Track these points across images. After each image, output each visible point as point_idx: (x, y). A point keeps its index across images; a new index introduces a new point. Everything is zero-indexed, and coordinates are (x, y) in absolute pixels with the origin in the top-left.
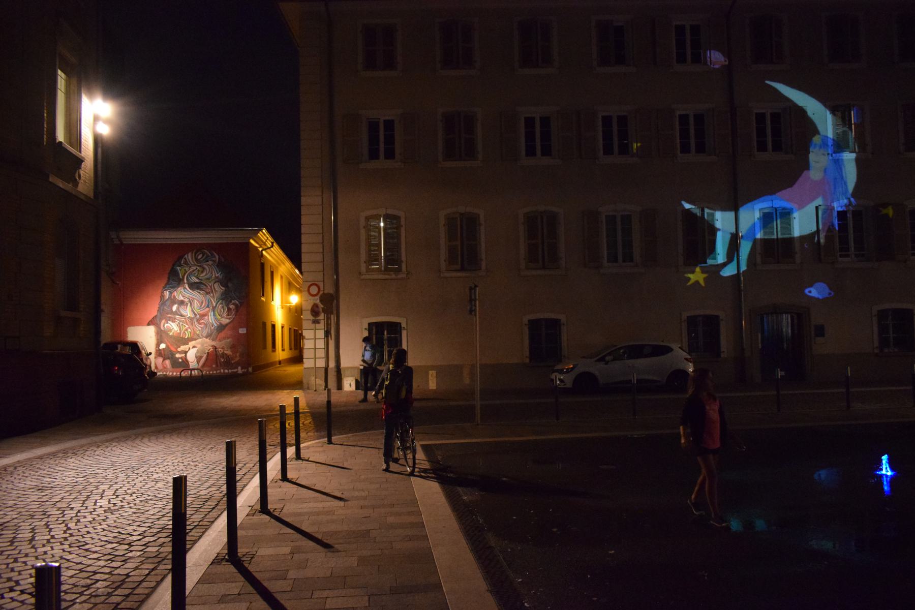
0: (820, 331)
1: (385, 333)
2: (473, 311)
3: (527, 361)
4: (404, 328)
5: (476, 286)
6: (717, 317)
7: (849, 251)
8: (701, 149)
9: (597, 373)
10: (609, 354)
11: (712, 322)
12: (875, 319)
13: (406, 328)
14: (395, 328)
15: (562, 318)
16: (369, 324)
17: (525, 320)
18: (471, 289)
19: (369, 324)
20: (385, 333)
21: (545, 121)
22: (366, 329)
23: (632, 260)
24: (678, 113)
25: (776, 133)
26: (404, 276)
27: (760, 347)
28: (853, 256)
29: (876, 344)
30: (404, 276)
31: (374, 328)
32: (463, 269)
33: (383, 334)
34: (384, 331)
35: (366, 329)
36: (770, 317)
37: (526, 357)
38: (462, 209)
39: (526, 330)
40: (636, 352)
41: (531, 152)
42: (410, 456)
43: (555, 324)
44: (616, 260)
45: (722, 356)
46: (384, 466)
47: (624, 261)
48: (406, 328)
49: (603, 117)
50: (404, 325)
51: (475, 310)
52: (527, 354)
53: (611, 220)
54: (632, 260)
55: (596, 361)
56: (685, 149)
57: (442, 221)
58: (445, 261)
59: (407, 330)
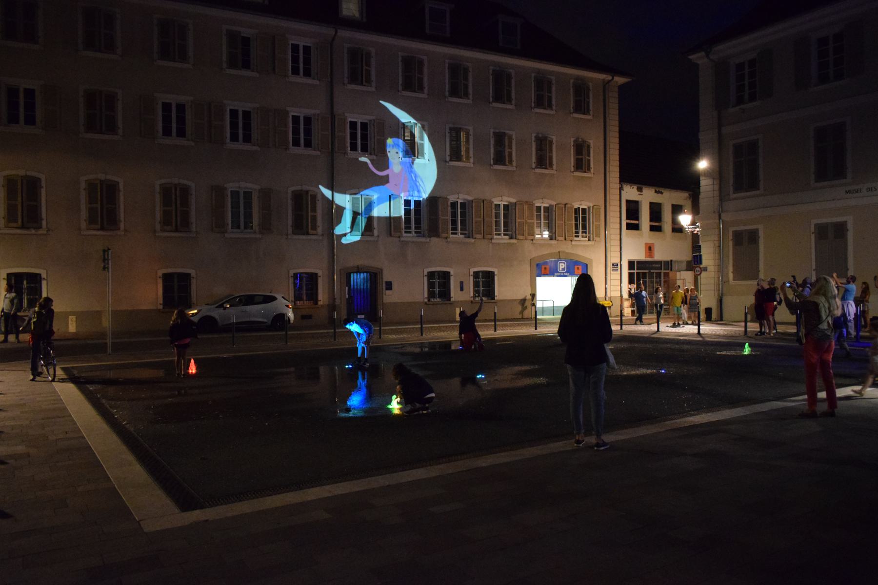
0: (389, 286)
1: (25, 282)
2: (106, 268)
3: (161, 307)
4: (44, 278)
5: (109, 249)
6: (316, 274)
7: (411, 229)
8: (308, 144)
9: (217, 317)
10: (227, 302)
11: (313, 278)
12: (426, 278)
13: (46, 278)
14: (35, 279)
15: (193, 272)
16: (9, 275)
17: (160, 273)
18: (104, 251)
19: (8, 275)
20: (25, 282)
21: (181, 108)
22: (4, 279)
24: (291, 114)
25: (364, 137)
26: (45, 232)
27: (347, 297)
28: (414, 233)
29: (426, 296)
30: (45, 232)
31: (13, 278)
32: (102, 228)
33: (22, 283)
34: (23, 281)
35: (4, 279)
36: (358, 276)
37: (160, 304)
38: (102, 177)
40: (250, 300)
41: (167, 132)
42: (51, 371)
43: (185, 278)
44: (239, 227)
46: (31, 377)
48: (46, 278)
49: (231, 110)
50: (44, 276)
51: (108, 268)
52: (162, 302)
53: (235, 194)
55: (217, 307)
56: (296, 143)
57: (83, 185)
59: (47, 280)
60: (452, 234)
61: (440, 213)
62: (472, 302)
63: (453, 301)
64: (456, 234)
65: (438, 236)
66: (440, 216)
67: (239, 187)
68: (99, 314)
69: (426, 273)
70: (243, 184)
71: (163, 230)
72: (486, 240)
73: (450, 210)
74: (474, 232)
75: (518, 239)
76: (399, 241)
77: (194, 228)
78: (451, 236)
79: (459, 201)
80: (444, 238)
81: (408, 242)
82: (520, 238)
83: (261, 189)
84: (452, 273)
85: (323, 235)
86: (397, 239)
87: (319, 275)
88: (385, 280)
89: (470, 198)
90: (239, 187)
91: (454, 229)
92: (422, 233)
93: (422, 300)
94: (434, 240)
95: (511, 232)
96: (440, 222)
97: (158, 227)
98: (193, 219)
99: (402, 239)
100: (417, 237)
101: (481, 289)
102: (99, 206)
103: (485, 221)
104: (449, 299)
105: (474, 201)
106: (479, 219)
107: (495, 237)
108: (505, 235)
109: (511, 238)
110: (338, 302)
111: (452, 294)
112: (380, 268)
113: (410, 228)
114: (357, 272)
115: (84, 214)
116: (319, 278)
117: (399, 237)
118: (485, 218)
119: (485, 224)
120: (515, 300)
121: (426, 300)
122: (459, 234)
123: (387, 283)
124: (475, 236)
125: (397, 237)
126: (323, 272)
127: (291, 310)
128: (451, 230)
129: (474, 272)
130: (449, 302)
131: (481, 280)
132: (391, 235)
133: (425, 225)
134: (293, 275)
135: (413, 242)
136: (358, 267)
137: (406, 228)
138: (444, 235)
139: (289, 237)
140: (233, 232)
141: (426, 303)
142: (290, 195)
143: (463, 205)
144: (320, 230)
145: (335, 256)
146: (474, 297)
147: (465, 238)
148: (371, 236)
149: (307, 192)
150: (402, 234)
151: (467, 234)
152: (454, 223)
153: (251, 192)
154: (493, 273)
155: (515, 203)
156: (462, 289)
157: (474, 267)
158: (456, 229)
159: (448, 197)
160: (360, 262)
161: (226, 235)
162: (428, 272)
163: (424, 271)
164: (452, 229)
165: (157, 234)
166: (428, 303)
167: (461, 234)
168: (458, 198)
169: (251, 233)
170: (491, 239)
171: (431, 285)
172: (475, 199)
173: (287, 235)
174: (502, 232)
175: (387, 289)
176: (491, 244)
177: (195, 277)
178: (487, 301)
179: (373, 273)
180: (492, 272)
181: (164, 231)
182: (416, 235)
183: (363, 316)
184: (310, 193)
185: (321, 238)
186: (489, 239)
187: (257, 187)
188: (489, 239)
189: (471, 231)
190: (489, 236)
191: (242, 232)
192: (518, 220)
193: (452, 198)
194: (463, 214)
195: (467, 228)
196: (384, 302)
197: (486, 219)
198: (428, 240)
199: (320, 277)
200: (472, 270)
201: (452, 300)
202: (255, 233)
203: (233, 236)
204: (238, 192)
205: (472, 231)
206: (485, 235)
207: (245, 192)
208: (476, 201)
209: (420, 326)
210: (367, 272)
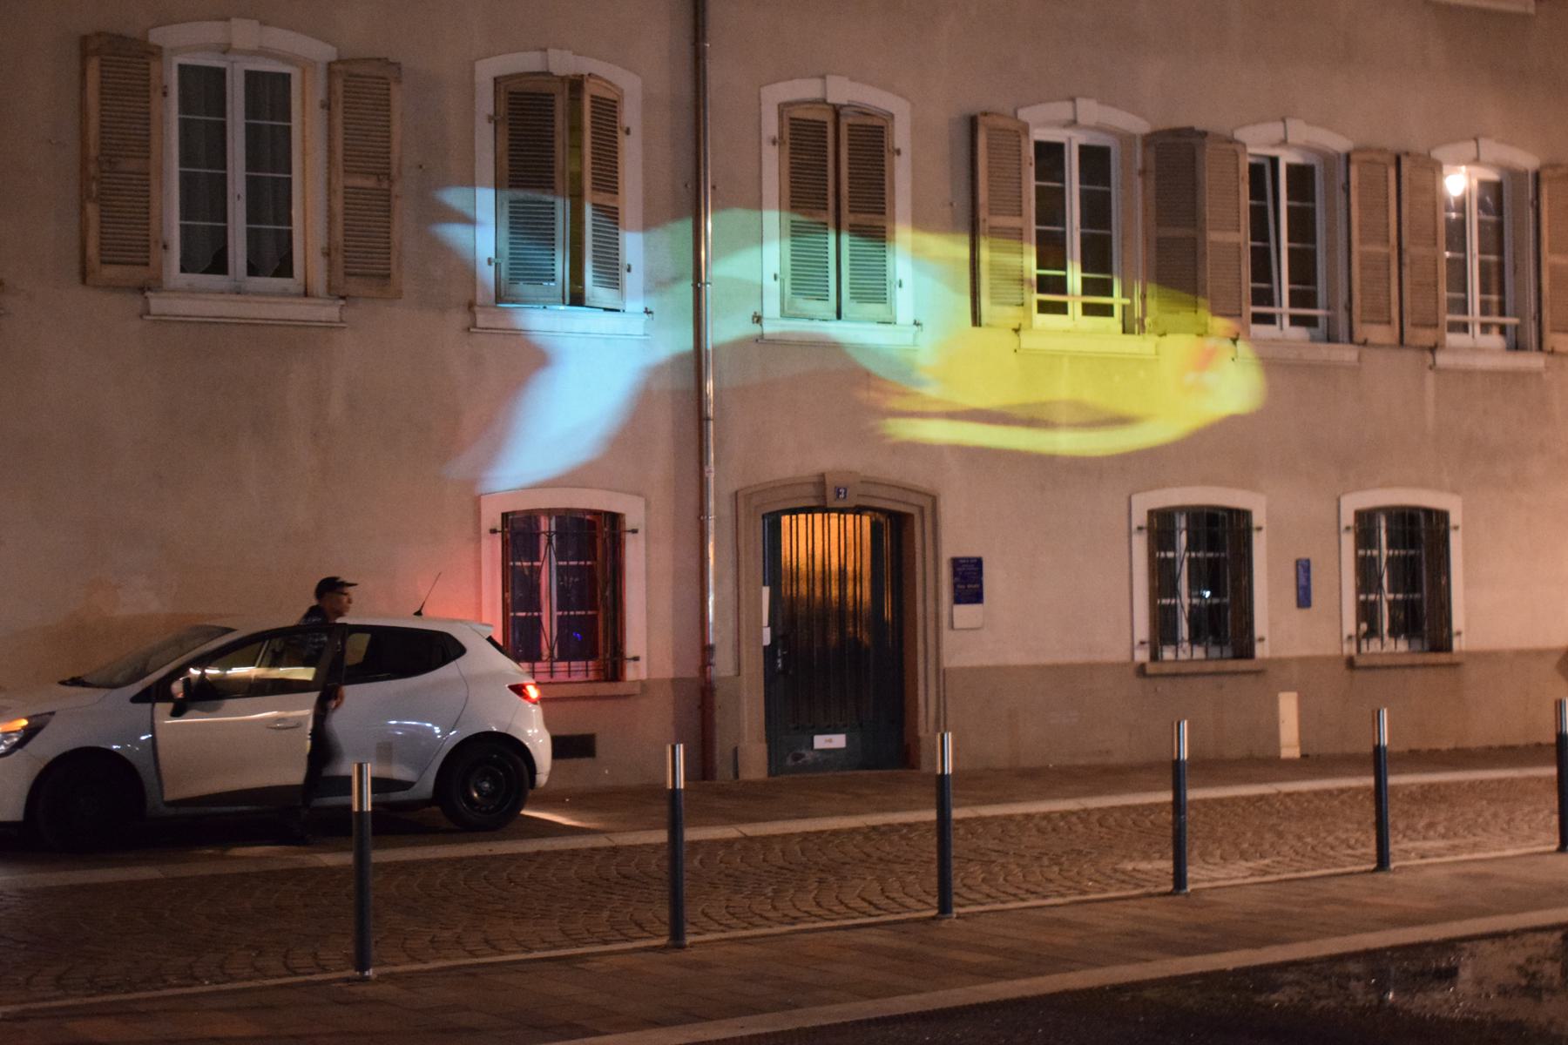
6: (615, 519)
12: (1140, 544)
23: (284, 268)
27: (767, 641)
29: (1142, 630)
44: (219, 265)
45: (632, 673)
47: (253, 270)
54: (284, 268)
55: (136, 699)
62: (1350, 663)
63: (1264, 661)
67: (226, 50)
70: (244, 33)
72: (1409, 356)
75: (1552, 352)
79: (1287, 158)
81: (1054, 357)
82: (1558, 348)
83: (340, 61)
84: (1258, 519)
87: (630, 523)
88: (949, 551)
89: (1338, 143)
90: (226, 50)
93: (1119, 654)
95: (1516, 316)
101: (1387, 596)
103: (1407, 259)
104: (1244, 650)
105: (1353, 157)
106: (1377, 249)
107: (1453, 339)
108: (1485, 328)
109: (1517, 346)
110: (723, 665)
111: (1260, 627)
112: (924, 485)
114: (809, 510)
116: (629, 537)
118: (1405, 244)
119: (1406, 271)
120: (1540, 654)
121: (1142, 656)
122: (1286, 321)
123: (956, 563)
124: (1358, 337)
127: (536, 712)
128: (1255, 302)
130: (1243, 665)
131: (1384, 552)
134: (498, 525)
135: (1076, 358)
136: (821, 481)
139: (482, 320)
140: (192, 291)
141: (1141, 670)
142: (485, 103)
143: (1301, 177)
146: (1359, 638)
147: (1313, 339)
149: (576, 85)
151: (1322, 323)
152: (1262, 266)
153: (286, 78)
154: (1443, 516)
155: (1537, 176)
156: (1304, 600)
157: (1360, 487)
159: (1240, 135)
160: (829, 459)
161: (158, 303)
162: (1151, 513)
166: (1151, 669)
167: (1296, 321)
168: (1284, 142)
169: (285, 294)
170: (1433, 349)
171: (1162, 578)
172: (1357, 150)
174: (1475, 315)
175: (959, 599)
176: (1430, 377)
178: (1419, 659)
179: (891, 514)
180: (1429, 512)
183: (838, 741)
184: (590, 89)
186: (1422, 348)
187: (324, 52)
188: (1422, 348)
190: (1426, 336)
191: (238, 292)
192: (1548, 258)
193: (1258, 141)
194: (1302, 225)
197: (1411, 251)
199: (635, 531)
200: (1354, 502)
201: (1261, 651)
204: (220, 74)
205: (1349, 309)
206: (1407, 328)
207: (252, 78)
208: (1366, 156)
209: (1167, 797)
210: (858, 510)
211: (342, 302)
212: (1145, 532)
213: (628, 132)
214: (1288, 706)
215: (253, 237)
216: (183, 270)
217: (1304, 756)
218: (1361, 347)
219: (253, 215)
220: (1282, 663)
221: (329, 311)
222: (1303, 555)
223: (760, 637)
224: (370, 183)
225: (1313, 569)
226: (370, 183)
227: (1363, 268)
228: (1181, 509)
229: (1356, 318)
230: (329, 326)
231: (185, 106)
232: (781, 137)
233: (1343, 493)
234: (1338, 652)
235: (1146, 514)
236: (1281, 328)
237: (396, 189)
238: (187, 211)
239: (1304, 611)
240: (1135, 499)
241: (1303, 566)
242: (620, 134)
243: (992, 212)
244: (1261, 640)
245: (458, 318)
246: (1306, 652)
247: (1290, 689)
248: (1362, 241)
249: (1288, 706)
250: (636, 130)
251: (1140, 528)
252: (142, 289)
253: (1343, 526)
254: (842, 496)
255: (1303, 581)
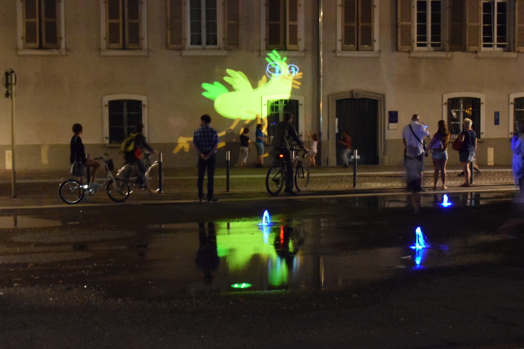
0: (394, 117)
3: (107, 141)
15: (144, 99)
17: (106, 100)
23: (215, 43)
28: (430, 46)
32: (41, 48)
39: (106, 111)
44: (199, 43)
47: (208, 44)
58: (22, 38)
60: (485, 46)
61: (467, 20)
63: (483, 139)
64: (490, 46)
65: (464, 49)
66: (467, 22)
68: (37, 148)
69: (445, 100)
71: (108, 48)
73: (481, 13)
74: (516, 43)
76: (408, 57)
77: (145, 43)
78: (483, 49)
80: (472, 52)
81: (420, 58)
85: (305, 50)
86: (407, 55)
87: (300, 103)
91: (488, 40)
92: (442, 46)
94: (458, 55)
96: (467, 31)
97: (104, 44)
98: (144, 32)
99: (412, 55)
100: (435, 51)
102: (37, 20)
112: (382, 93)
113: (425, 39)
115: (21, 30)
117: (409, 52)
122: (496, 46)
123: (390, 113)
124: (517, 50)
125: (405, 52)
126: (305, 97)
128: (484, 41)
129: (516, 100)
132: (397, 49)
133: (445, 34)
135: (427, 58)
137: (419, 39)
138: (473, 48)
139: (262, 54)
144: (301, 45)
145: (322, 79)
147: (504, 51)
148: (370, 51)
150: (412, 47)
156: (497, 122)
157: (516, 92)
158: (490, 40)
161: (184, 53)
162: (449, 99)
163: (442, 97)
164: (485, 40)
165: (102, 53)
167: (498, 46)
169: (215, 49)
173: (259, 51)
175: (391, 121)
177: (146, 104)
181: (110, 49)
182: (432, 49)
185: (303, 54)
189: (512, 42)
191: (204, 49)
194: (502, 20)
195: (507, 38)
196: (387, 138)
198: (450, 54)
199: (301, 105)
202: (220, 49)
203: (190, 53)
205: (514, 42)
211: (227, 51)
212: (447, 104)
213: (300, 6)
214: (491, 152)
215: (207, 36)
216: (191, 44)
217: (495, 165)
218: (518, 53)
219: (208, 31)
220: (490, 140)
221: (225, 53)
222: (497, 110)
223: (335, 131)
224: (233, 22)
225: (500, 114)
226: (233, 22)
227: (519, 31)
228: (461, 98)
229: (516, 45)
230: (225, 57)
231: (191, 6)
232: (342, 4)
233: (511, 94)
234: (508, 137)
235: (447, 100)
236: (494, 48)
237: (240, 23)
238: (192, 30)
239: (496, 126)
240: (444, 95)
241: (497, 114)
242: (298, 7)
243: (402, 21)
244: (483, 133)
245: (256, 54)
246: (497, 137)
247: (491, 146)
248: (519, 23)
249: (491, 152)
250: (303, 5)
251: (445, 103)
252: (180, 50)
253: (510, 102)
254: (357, 95)
255: (496, 118)
